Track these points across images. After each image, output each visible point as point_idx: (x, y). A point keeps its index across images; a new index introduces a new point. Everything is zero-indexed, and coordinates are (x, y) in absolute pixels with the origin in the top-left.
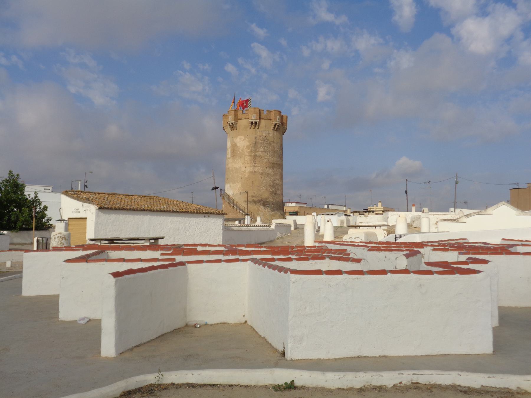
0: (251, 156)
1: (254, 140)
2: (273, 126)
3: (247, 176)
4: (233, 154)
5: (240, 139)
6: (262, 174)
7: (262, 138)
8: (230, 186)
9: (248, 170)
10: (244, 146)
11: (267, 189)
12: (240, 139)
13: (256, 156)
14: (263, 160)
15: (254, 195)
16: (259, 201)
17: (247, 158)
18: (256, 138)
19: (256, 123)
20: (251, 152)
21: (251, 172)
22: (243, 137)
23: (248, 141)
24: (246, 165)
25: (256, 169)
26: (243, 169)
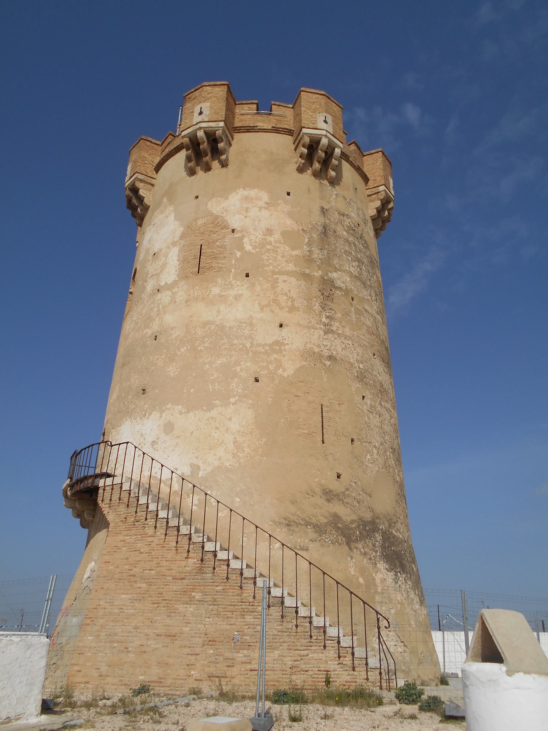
0: (307, 277)
1: (317, 219)
2: (378, 204)
3: (289, 368)
4: (200, 262)
6: (361, 377)
7: (347, 222)
8: (169, 428)
9: (296, 339)
10: (269, 232)
11: (386, 466)
12: (246, 199)
13: (331, 282)
14: (358, 312)
15: (336, 486)
16: (368, 528)
17: (291, 286)
18: (323, 211)
19: (329, 152)
20: (309, 260)
21: (312, 356)
22: (265, 196)
23: (290, 215)
24: (284, 316)
25: (337, 347)
26: (266, 334)
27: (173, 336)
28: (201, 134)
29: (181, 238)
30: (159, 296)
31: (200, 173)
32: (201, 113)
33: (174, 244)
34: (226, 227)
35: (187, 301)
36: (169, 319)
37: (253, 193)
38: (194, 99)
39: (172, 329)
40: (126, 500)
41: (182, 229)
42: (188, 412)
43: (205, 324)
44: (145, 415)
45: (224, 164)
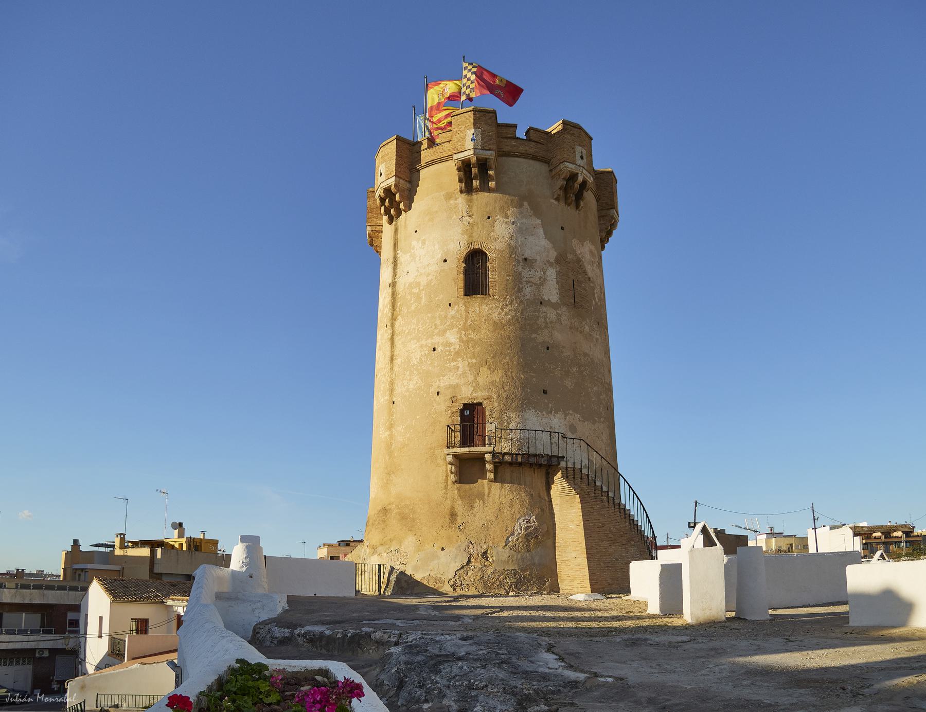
5: (591, 252)
27: (565, 354)
28: (580, 179)
29: (557, 261)
30: (543, 309)
31: (562, 204)
32: (582, 158)
33: (551, 265)
34: (585, 272)
35: (571, 328)
36: (558, 336)
37: (593, 248)
38: (573, 134)
39: (563, 347)
40: (586, 480)
41: (555, 253)
42: (583, 421)
43: (586, 355)
44: (551, 412)
45: (577, 207)
